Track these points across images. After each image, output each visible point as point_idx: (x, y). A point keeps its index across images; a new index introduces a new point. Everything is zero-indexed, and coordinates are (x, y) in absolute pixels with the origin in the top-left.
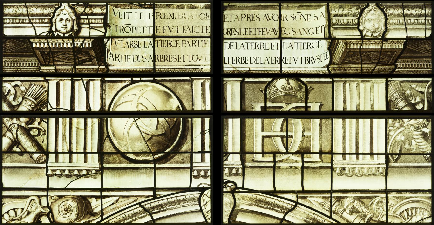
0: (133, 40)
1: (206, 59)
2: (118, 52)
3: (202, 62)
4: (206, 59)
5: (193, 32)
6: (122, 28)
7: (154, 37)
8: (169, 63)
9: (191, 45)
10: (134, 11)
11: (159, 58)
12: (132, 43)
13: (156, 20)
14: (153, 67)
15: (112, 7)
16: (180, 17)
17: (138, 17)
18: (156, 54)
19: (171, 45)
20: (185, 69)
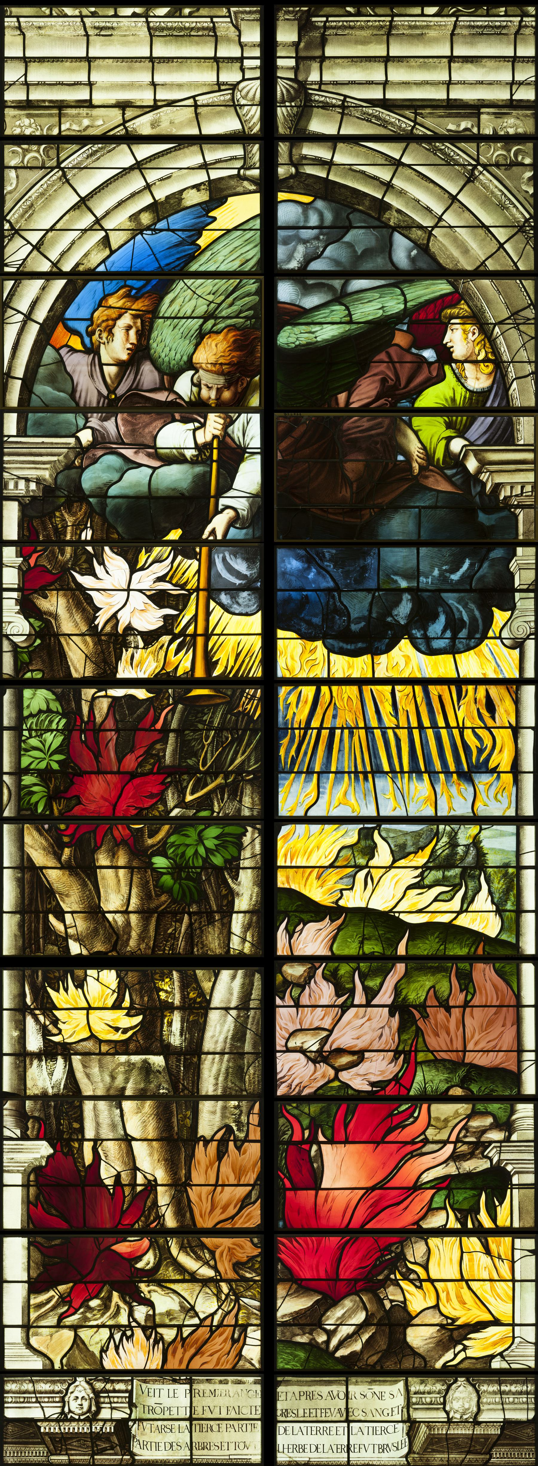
0: (165, 1423)
2: (146, 1438)
7: (191, 1419)
10: (166, 1387)
17: (171, 1394)
19: (212, 1430)
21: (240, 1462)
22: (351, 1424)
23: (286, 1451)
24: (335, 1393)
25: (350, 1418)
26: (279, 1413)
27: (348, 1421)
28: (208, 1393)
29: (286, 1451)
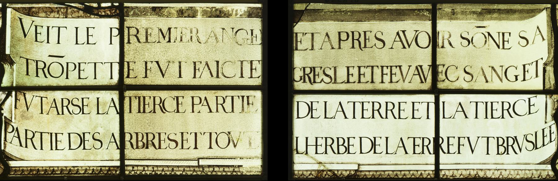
0: (70, 94)
1: (250, 144)
2: (32, 125)
3: (241, 150)
4: (250, 144)
5: (218, 77)
6: (41, 65)
7: (121, 87)
8: (160, 154)
9: (214, 109)
10: (71, 23)
11: (134, 141)
12: (66, 103)
13: (126, 46)
14: (118, 164)
15: (18, 15)
16: (186, 38)
17: (82, 38)
18: (127, 129)
19: (163, 109)
20: (199, 166)
21: (219, 172)
22: (443, 98)
23: (312, 150)
24: (410, 36)
25: (441, 86)
26: (298, 74)
27: (436, 91)
28: (155, 35)
29: (312, 150)
